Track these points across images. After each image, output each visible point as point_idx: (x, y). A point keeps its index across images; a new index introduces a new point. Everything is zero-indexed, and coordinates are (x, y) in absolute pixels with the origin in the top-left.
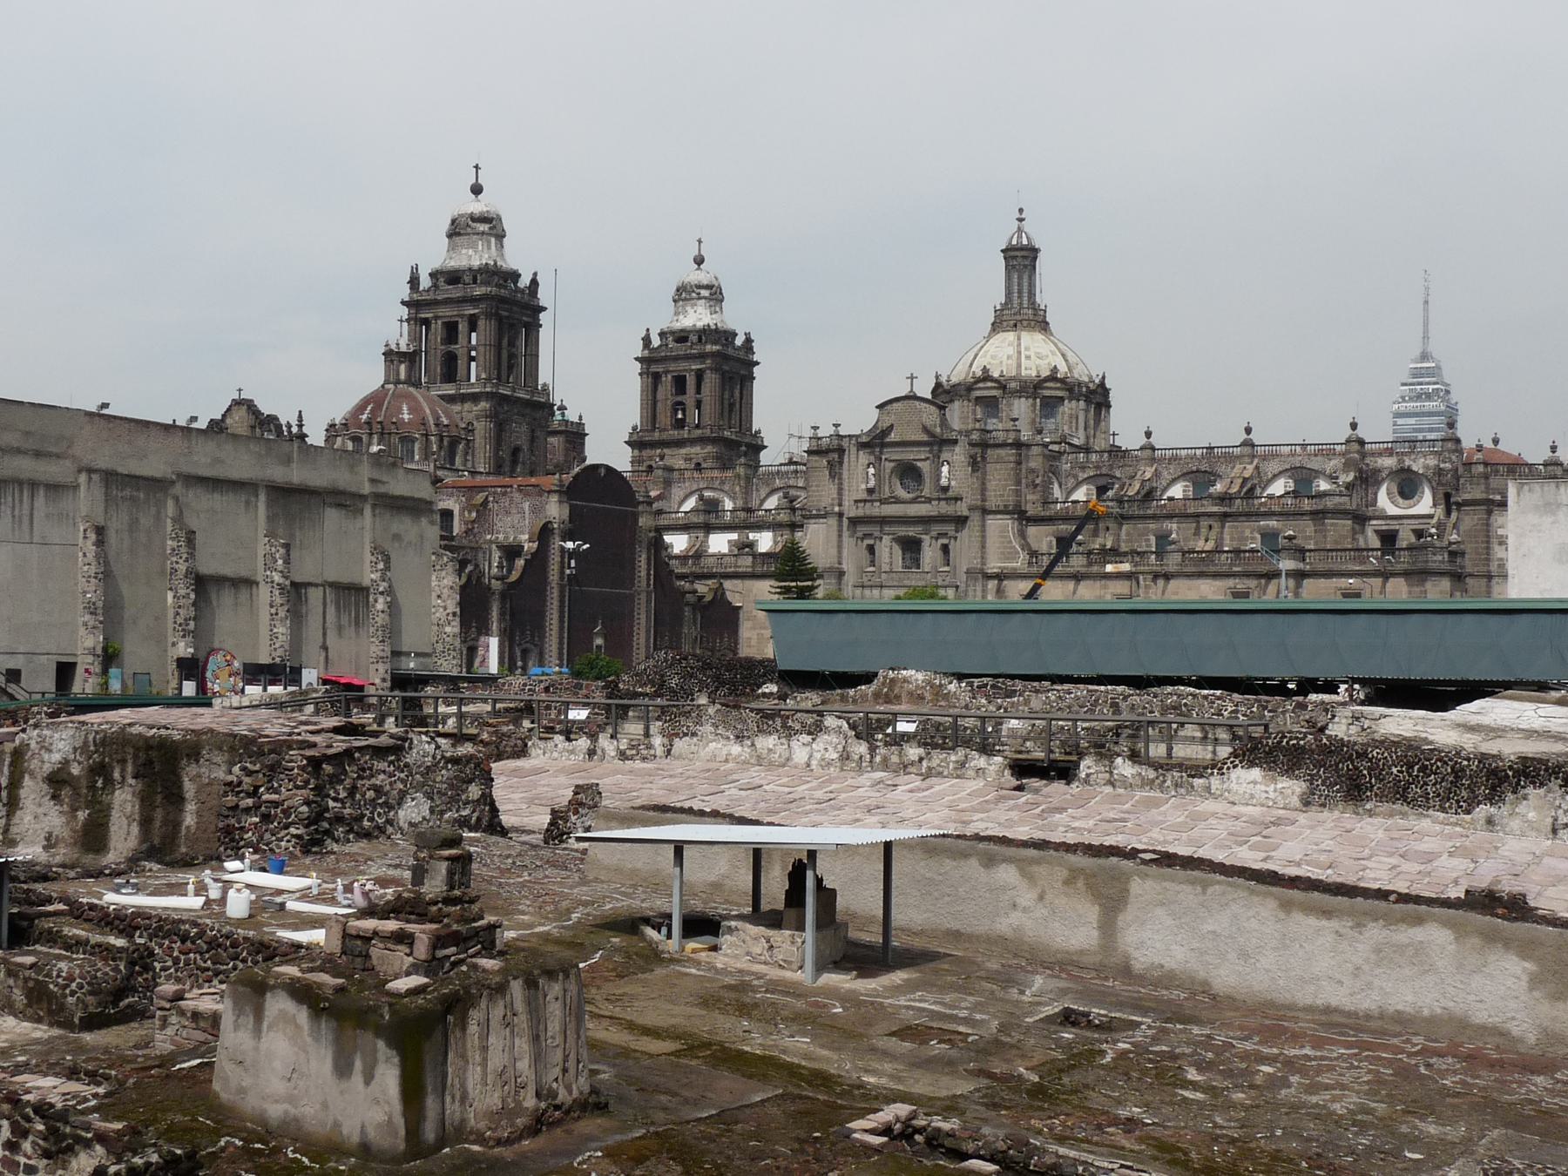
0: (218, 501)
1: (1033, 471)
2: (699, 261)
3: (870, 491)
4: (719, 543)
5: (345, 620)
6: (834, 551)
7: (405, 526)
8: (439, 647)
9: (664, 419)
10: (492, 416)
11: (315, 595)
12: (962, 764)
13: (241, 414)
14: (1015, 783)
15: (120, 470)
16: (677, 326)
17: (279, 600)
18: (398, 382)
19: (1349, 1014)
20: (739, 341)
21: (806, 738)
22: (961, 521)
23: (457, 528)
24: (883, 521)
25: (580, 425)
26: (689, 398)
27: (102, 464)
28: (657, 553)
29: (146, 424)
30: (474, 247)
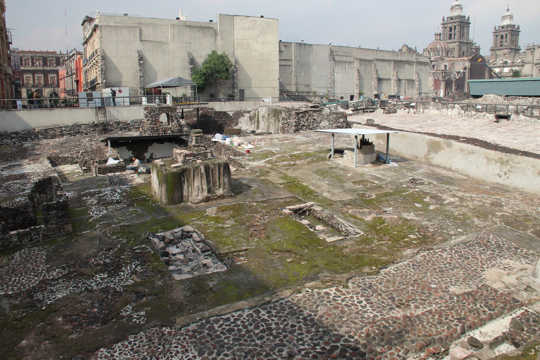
0: (383, 64)
4: (506, 70)
5: (409, 87)
7: (423, 67)
8: (430, 92)
9: (498, 45)
10: (459, 46)
11: (403, 82)
12: (484, 116)
13: (405, 48)
14: (496, 120)
15: (363, 58)
16: (502, 25)
17: (395, 83)
19: (502, 185)
21: (451, 109)
23: (448, 68)
25: (479, 47)
26: (504, 40)
27: (359, 57)
28: (490, 73)
29: (369, 49)
30: (455, 11)
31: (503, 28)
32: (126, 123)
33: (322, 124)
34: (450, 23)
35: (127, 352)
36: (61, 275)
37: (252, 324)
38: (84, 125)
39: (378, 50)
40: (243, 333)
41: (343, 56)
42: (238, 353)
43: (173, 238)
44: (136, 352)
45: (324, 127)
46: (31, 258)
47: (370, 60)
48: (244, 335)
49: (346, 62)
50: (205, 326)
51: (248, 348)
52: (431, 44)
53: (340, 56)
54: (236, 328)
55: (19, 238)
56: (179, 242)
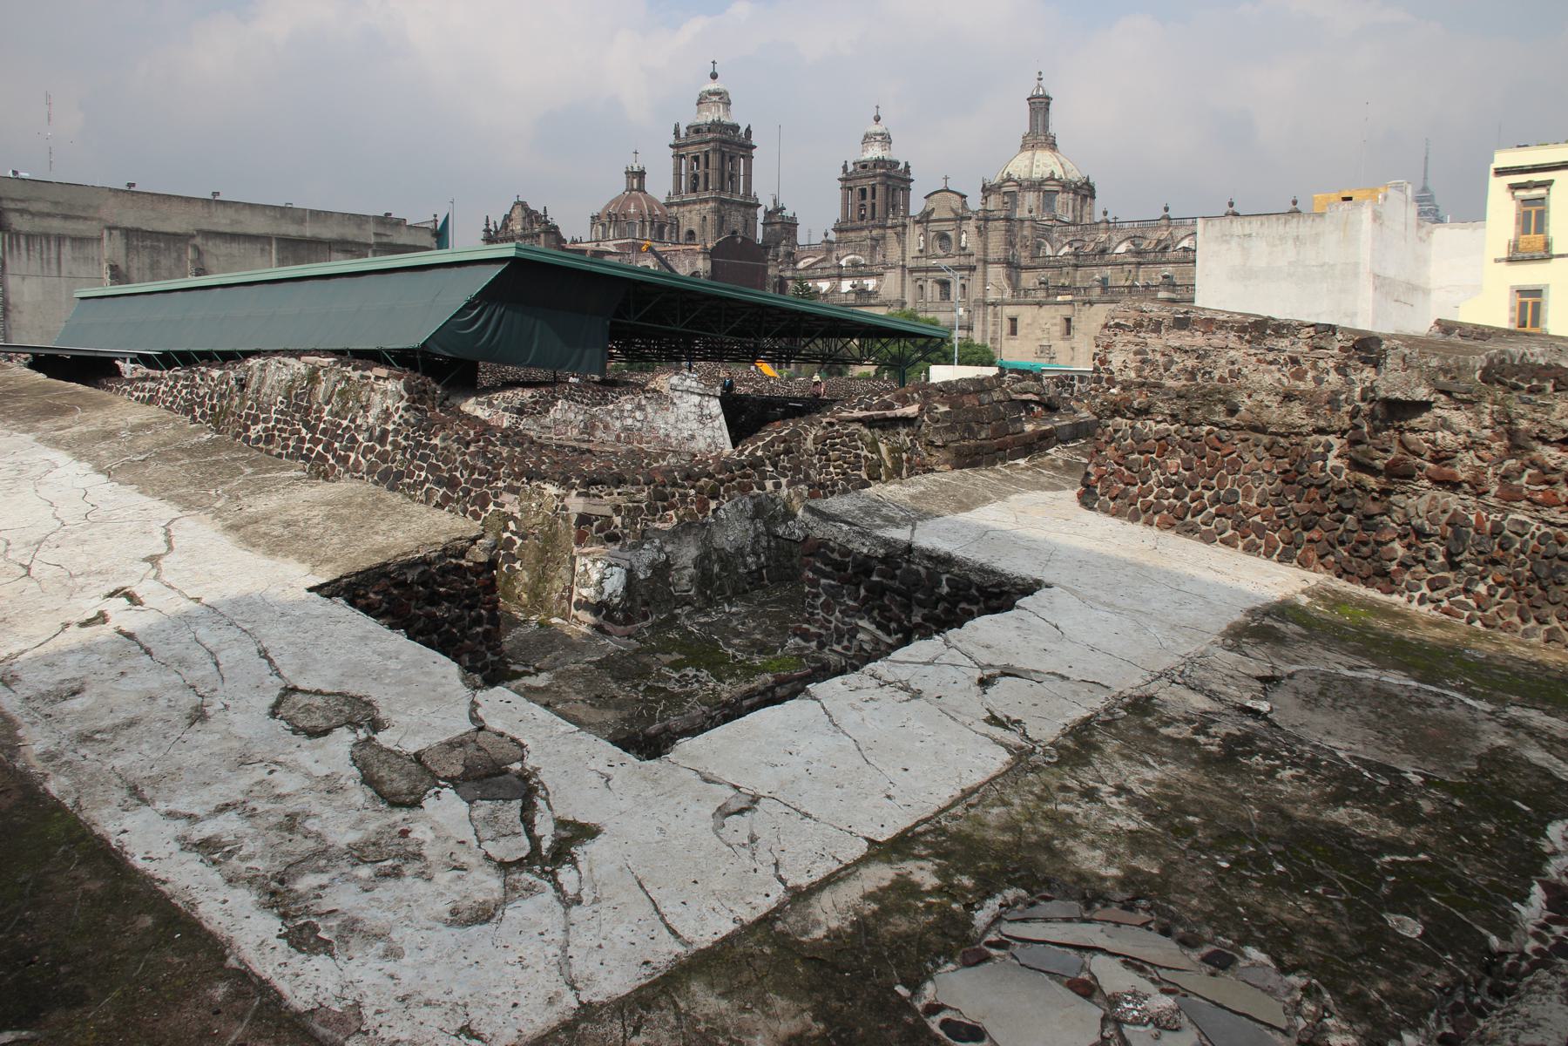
1: (1025, 237)
2: (877, 119)
3: (921, 251)
4: (846, 285)
6: (899, 290)
10: (717, 211)
15: (144, 228)
16: (863, 158)
18: (633, 190)
20: (902, 166)
22: (972, 269)
24: (927, 270)
25: (794, 218)
26: (868, 201)
29: (169, 197)
30: (709, 110)
31: (864, 167)
34: (693, 144)
39: (214, 202)
41: (48, 215)
47: (175, 235)
49: (60, 239)
52: (612, 202)
53: (33, 214)
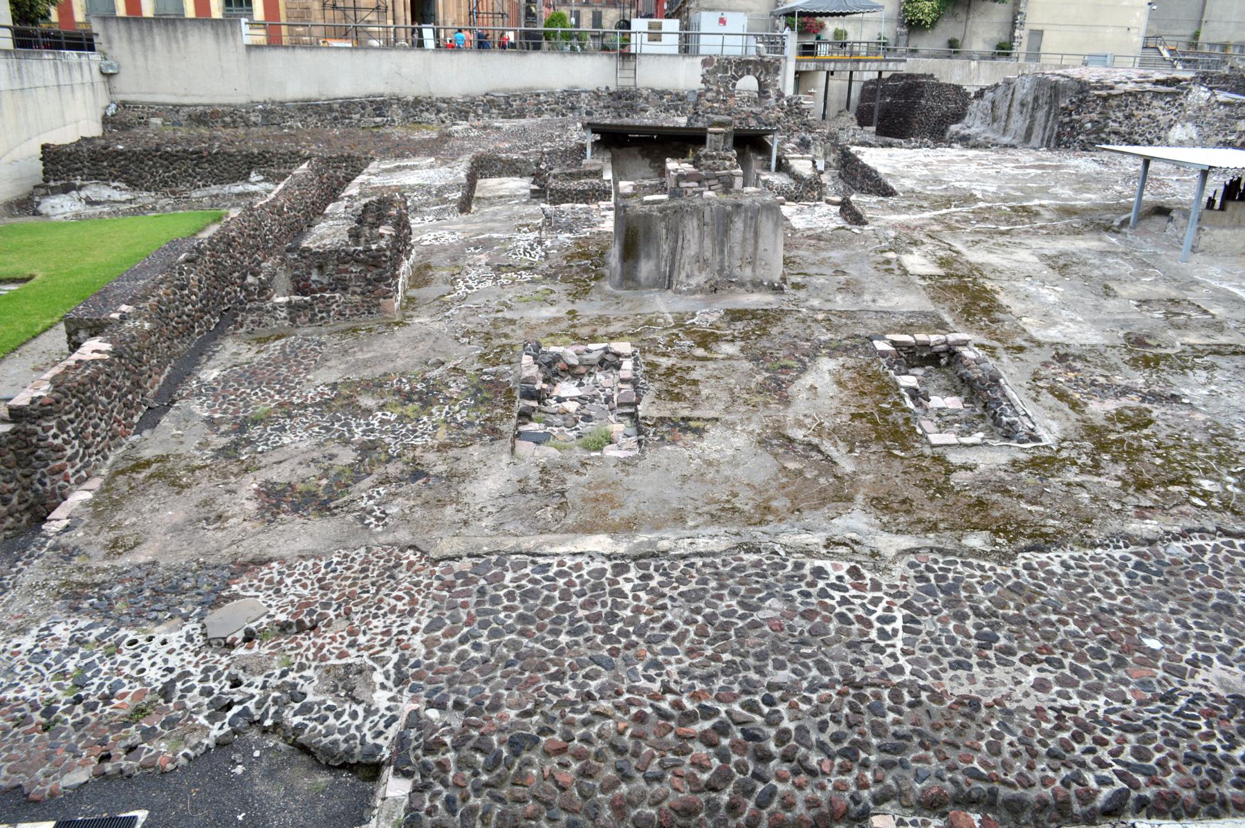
32: (677, 95)
33: (1177, 133)
35: (309, 582)
36: (318, 399)
37: (585, 594)
38: (586, 92)
40: (551, 608)
42: (505, 650)
43: (576, 363)
44: (321, 588)
45: (1181, 143)
46: (296, 356)
48: (548, 614)
50: (489, 570)
51: (531, 645)
54: (546, 593)
55: (290, 313)
56: (590, 374)
